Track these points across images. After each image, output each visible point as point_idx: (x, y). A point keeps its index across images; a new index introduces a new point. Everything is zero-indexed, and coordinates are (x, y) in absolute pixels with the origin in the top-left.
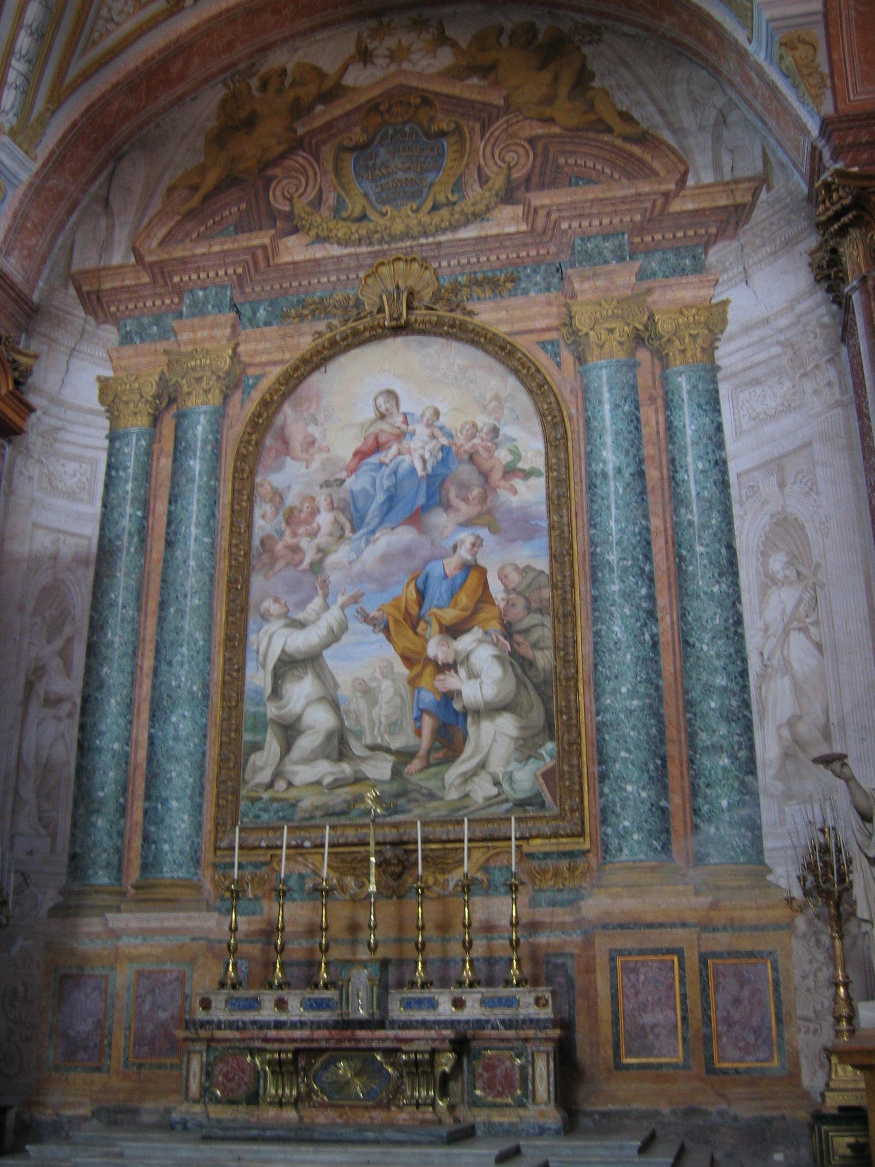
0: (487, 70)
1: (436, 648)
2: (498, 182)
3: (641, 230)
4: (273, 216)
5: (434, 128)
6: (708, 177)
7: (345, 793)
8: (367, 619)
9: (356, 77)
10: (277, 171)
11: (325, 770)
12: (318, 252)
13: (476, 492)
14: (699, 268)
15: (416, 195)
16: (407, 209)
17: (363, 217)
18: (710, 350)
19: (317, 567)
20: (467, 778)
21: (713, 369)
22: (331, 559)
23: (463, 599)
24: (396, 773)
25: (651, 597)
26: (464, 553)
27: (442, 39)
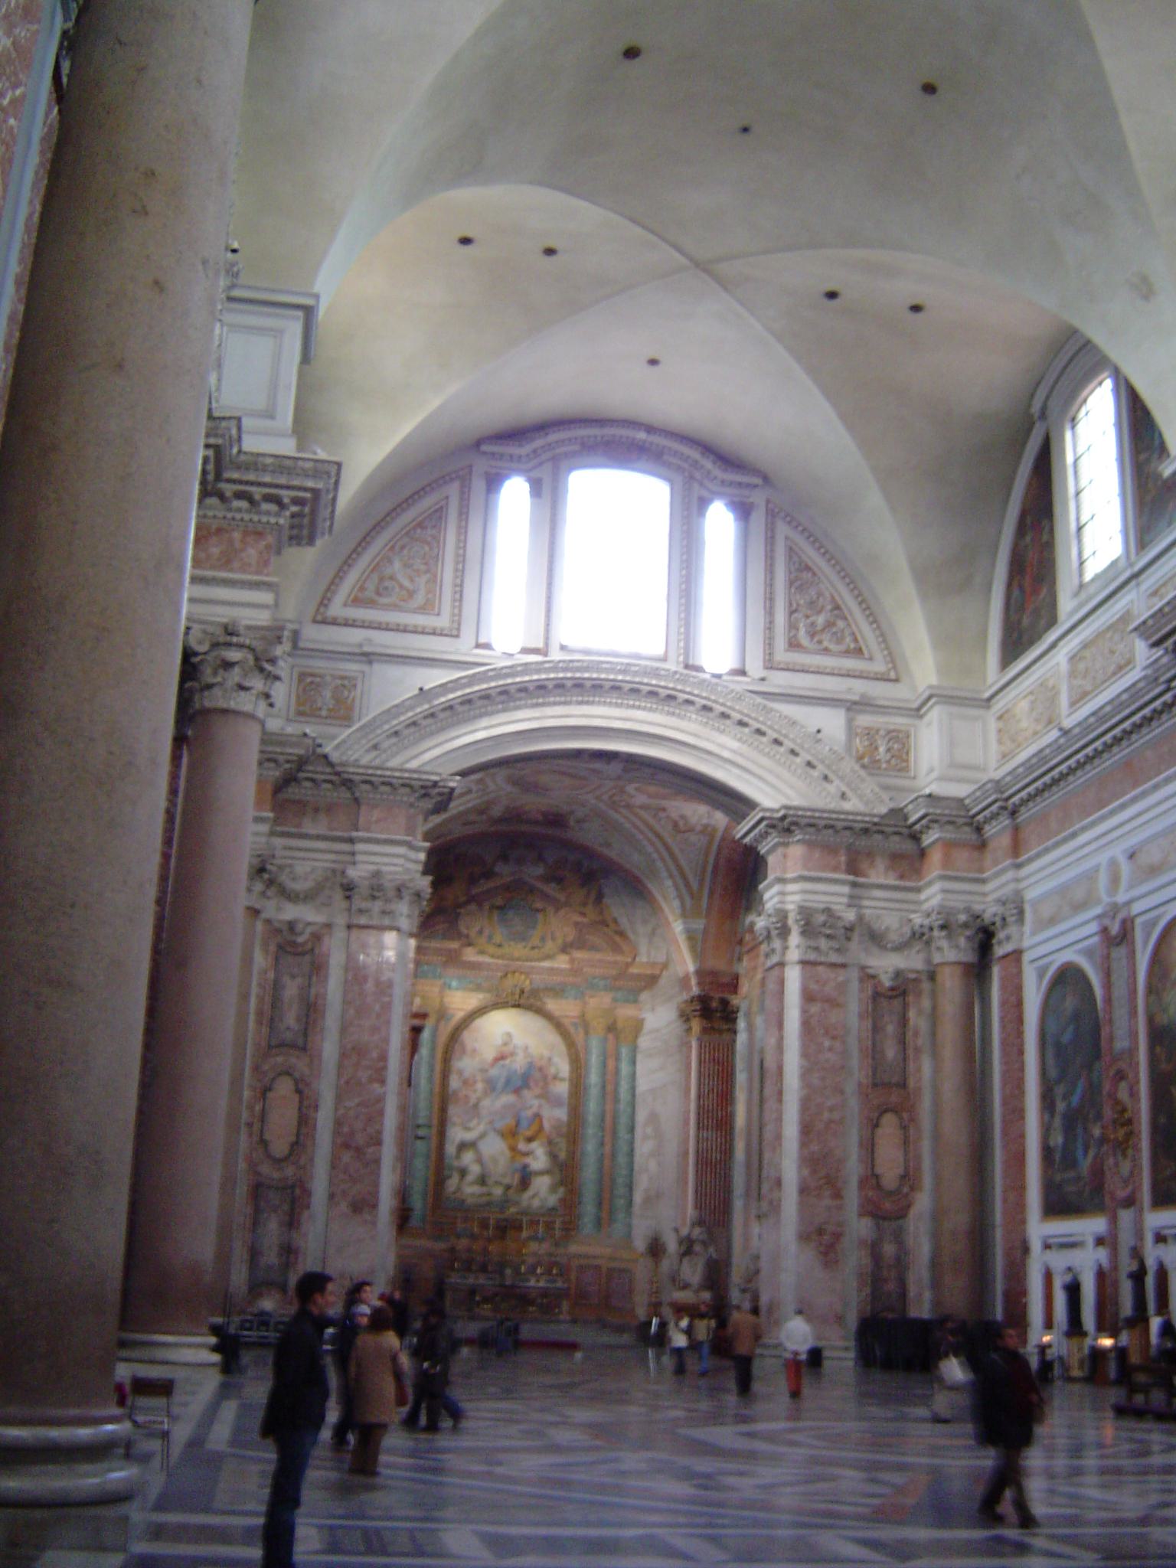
0: (559, 880)
1: (522, 1146)
2: (560, 941)
3: (616, 978)
4: (459, 935)
5: (534, 906)
6: (644, 959)
7: (484, 1199)
8: (495, 1130)
9: (501, 868)
10: (462, 911)
11: (476, 1189)
12: (480, 958)
13: (541, 1084)
14: (636, 1001)
15: (524, 939)
16: (520, 946)
17: (500, 946)
18: (636, 1037)
19: (476, 1106)
20: (534, 1196)
21: (634, 1050)
22: (481, 1104)
23: (535, 1127)
24: (505, 1194)
25: (603, 1136)
26: (534, 1110)
27: (541, 859)
